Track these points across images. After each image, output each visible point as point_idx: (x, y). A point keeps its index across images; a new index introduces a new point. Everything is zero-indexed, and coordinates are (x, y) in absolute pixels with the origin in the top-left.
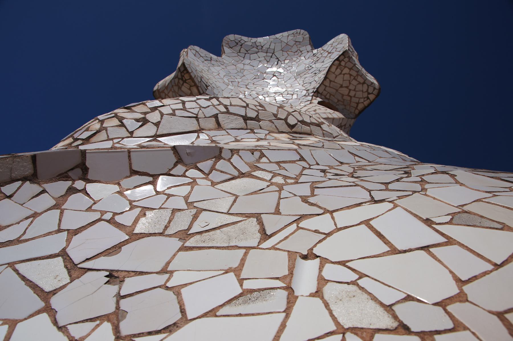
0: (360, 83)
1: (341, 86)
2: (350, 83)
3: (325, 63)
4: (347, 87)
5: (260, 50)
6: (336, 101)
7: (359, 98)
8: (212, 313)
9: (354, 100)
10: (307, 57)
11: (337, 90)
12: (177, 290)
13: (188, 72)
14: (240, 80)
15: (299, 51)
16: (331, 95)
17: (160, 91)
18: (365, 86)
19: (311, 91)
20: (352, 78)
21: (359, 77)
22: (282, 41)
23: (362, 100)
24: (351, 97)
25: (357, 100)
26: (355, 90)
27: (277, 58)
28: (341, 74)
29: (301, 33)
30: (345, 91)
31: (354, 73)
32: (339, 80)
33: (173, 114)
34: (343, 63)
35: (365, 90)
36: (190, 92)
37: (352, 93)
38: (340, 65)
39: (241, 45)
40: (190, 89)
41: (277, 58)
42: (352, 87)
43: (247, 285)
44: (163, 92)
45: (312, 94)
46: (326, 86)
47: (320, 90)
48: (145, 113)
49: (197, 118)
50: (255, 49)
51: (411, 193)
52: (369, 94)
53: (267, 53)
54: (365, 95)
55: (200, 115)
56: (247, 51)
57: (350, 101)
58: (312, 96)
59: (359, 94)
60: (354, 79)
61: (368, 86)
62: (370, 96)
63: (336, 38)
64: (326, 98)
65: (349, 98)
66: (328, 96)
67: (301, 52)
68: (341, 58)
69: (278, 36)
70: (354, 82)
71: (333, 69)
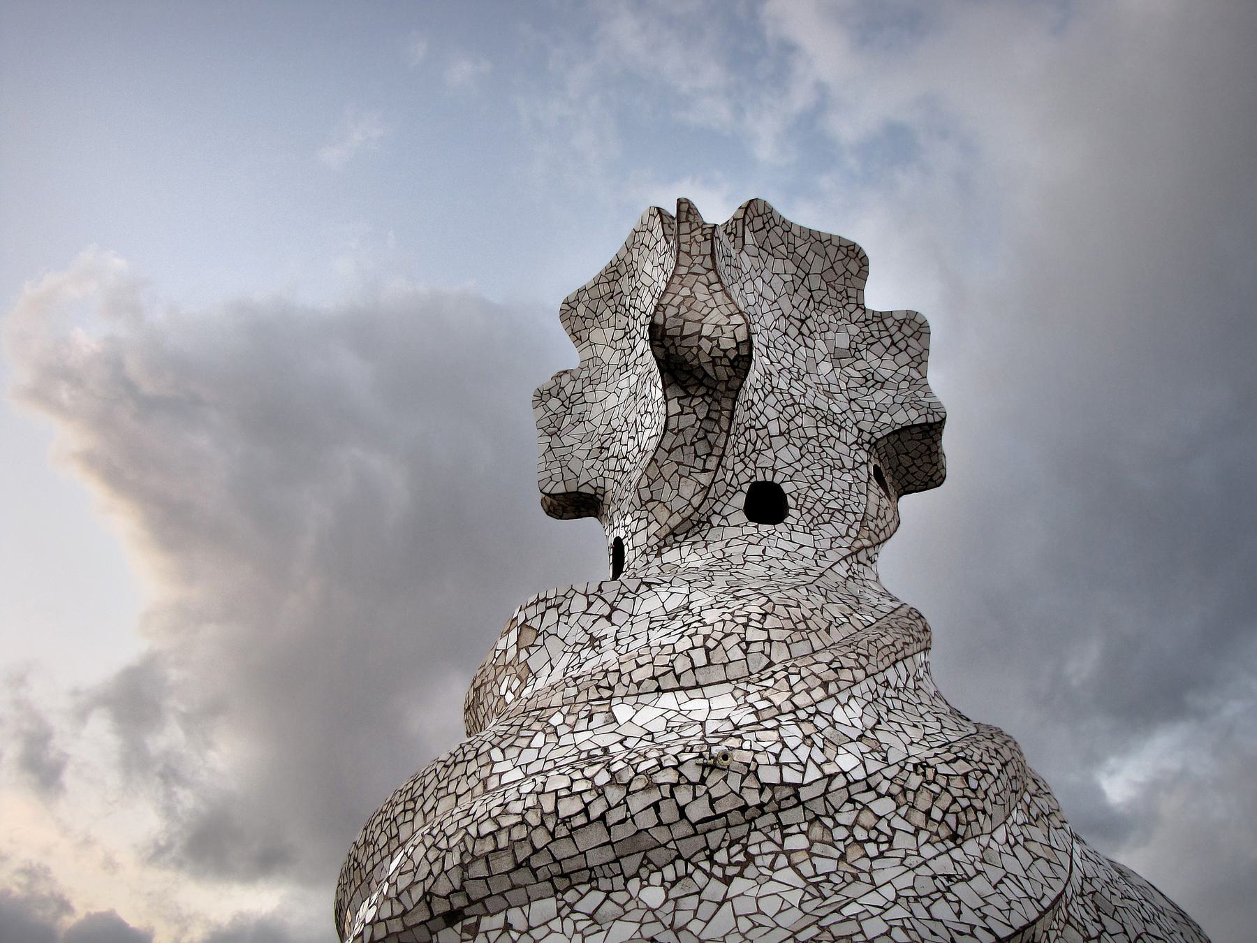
1: (907, 454)
3: (885, 364)
4: (913, 459)
9: (909, 478)
10: (855, 317)
11: (898, 454)
19: (866, 437)
30: (906, 461)
31: (933, 449)
32: (911, 446)
34: (932, 433)
36: (726, 378)
38: (928, 432)
40: (729, 377)
41: (810, 291)
44: (672, 337)
47: (880, 445)
50: (783, 249)
52: (931, 480)
67: (848, 297)
70: (926, 459)
71: (914, 431)
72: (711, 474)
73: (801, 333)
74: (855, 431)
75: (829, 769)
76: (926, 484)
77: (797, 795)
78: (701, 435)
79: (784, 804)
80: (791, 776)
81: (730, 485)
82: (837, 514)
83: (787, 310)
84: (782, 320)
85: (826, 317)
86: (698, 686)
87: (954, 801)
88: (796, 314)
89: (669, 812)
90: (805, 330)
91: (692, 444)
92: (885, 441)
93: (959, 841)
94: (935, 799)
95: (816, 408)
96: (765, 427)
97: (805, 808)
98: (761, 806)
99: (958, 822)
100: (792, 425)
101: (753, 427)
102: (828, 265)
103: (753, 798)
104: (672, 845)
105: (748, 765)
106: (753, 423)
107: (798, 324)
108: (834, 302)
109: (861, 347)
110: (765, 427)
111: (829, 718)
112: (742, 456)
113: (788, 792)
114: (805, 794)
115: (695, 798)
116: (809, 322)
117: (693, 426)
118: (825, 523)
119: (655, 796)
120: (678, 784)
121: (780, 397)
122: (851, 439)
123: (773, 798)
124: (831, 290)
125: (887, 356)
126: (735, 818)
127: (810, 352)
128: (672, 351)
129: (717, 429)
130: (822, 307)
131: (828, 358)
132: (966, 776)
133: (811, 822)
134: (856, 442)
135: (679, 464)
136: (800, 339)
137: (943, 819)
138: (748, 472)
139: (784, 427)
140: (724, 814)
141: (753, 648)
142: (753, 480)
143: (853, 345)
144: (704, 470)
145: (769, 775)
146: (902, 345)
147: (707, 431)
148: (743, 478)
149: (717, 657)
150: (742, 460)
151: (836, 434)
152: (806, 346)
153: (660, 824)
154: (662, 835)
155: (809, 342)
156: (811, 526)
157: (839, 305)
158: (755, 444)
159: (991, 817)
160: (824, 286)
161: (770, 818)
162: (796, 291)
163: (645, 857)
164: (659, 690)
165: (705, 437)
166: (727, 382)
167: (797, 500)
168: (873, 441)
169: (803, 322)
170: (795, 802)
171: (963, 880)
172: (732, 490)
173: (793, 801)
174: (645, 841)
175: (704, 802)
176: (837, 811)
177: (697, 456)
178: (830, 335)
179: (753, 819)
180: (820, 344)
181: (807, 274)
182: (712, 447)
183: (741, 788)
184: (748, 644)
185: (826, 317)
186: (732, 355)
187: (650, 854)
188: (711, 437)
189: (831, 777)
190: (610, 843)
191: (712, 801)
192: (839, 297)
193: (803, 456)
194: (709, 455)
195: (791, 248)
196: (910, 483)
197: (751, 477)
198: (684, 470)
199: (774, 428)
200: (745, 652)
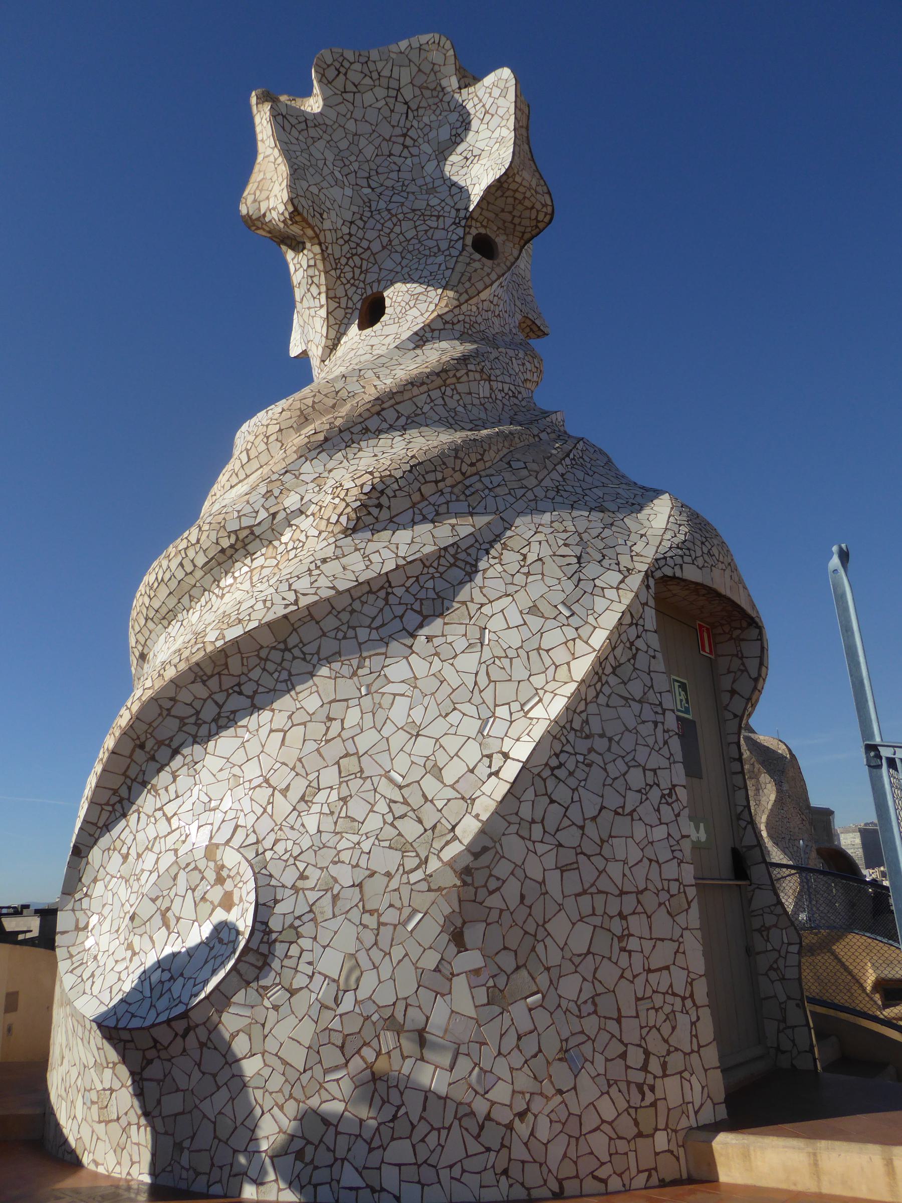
0: (527, 208)
1: (503, 211)
2: (514, 209)
4: (510, 213)
5: (377, 83)
6: (495, 229)
7: (526, 227)
8: (463, 652)
9: (518, 228)
12: (450, 643)
13: (299, 214)
14: (356, 165)
15: (439, 89)
16: (488, 220)
17: (254, 217)
18: (534, 211)
20: (517, 202)
21: (526, 200)
22: (410, 61)
23: (529, 229)
24: (515, 225)
25: (522, 229)
26: (520, 217)
27: (406, 103)
28: (502, 196)
29: (441, 44)
30: (508, 218)
32: (500, 203)
33: (395, 496)
34: (505, 185)
35: (533, 217)
37: (517, 221)
39: (345, 74)
41: (406, 103)
42: (516, 213)
43: (471, 641)
44: (258, 219)
45: (463, 223)
46: (482, 209)
48: (378, 498)
49: (410, 495)
50: (367, 81)
51: (519, 588)
52: (538, 222)
53: (388, 88)
54: (534, 223)
55: (411, 492)
56: (356, 86)
57: (514, 229)
58: (464, 227)
59: (526, 222)
60: (520, 203)
61: (538, 211)
62: (539, 224)
63: (499, 71)
64: (483, 226)
65: (512, 226)
66: (485, 223)
68: (502, 180)
69: (403, 44)
70: (520, 207)
72: (325, 307)
73: (405, 147)
74: (453, 212)
75: (272, 511)
76: (537, 227)
77: (252, 533)
78: (310, 282)
79: (247, 541)
80: (246, 522)
81: (347, 308)
82: (421, 297)
83: (386, 131)
84: (384, 144)
85: (426, 120)
86: (247, 476)
87: (347, 505)
88: (398, 131)
89: (189, 568)
90: (409, 142)
91: (309, 290)
92: (479, 210)
93: (350, 532)
94: (335, 508)
95: (414, 210)
96: (369, 248)
97: (261, 539)
98: (232, 546)
99: (348, 519)
100: (393, 236)
101: (353, 255)
102: (414, 69)
103: (225, 543)
104: (198, 584)
105: (220, 523)
106: (354, 251)
107: (401, 140)
108: (431, 101)
109: (459, 131)
110: (369, 248)
111: (297, 473)
112: (352, 281)
113: (247, 532)
114: (257, 531)
115: (197, 553)
116: (412, 133)
117: (303, 277)
118: (411, 308)
119: (179, 559)
120: (188, 547)
121: (378, 217)
122: (449, 221)
123: (237, 539)
124: (425, 92)
125: (484, 126)
126: (222, 558)
127: (416, 160)
128: (268, 229)
129: (317, 273)
130: (421, 111)
131: (433, 157)
132: (362, 486)
133: (267, 547)
134: (454, 223)
135: (309, 308)
136: (406, 153)
137: (338, 521)
138: (359, 291)
139: (385, 240)
140: (212, 558)
141: (272, 439)
142: (365, 295)
143: (454, 132)
144: (322, 306)
145: (233, 526)
146: (492, 111)
147: (311, 277)
148: (356, 298)
149: (253, 454)
150: (353, 285)
151: (434, 224)
152: (412, 156)
153: (187, 574)
154: (191, 580)
155: (415, 151)
156: (400, 316)
157: (437, 100)
158: (361, 267)
159: (389, 508)
160: (417, 92)
161: (242, 552)
162: (392, 111)
163: (190, 596)
164: (232, 487)
165: (313, 282)
166: (304, 233)
167: (391, 299)
168: (468, 215)
169: (405, 135)
170: (253, 537)
171: (337, 558)
172: (350, 311)
173: (251, 537)
174: (185, 587)
175: (201, 553)
176: (282, 535)
177: (314, 298)
178: (432, 135)
179: (232, 556)
180: (426, 148)
181: (398, 90)
182: (318, 287)
183: (217, 539)
184: (268, 438)
185: (426, 120)
186: (287, 215)
187: (191, 593)
188: (316, 280)
189: (274, 515)
190: (171, 593)
191: (205, 551)
192: (435, 93)
193: (403, 258)
194: (319, 294)
195: (375, 75)
196: (524, 233)
197: (362, 295)
198: (312, 311)
199: (376, 247)
200: (266, 444)
